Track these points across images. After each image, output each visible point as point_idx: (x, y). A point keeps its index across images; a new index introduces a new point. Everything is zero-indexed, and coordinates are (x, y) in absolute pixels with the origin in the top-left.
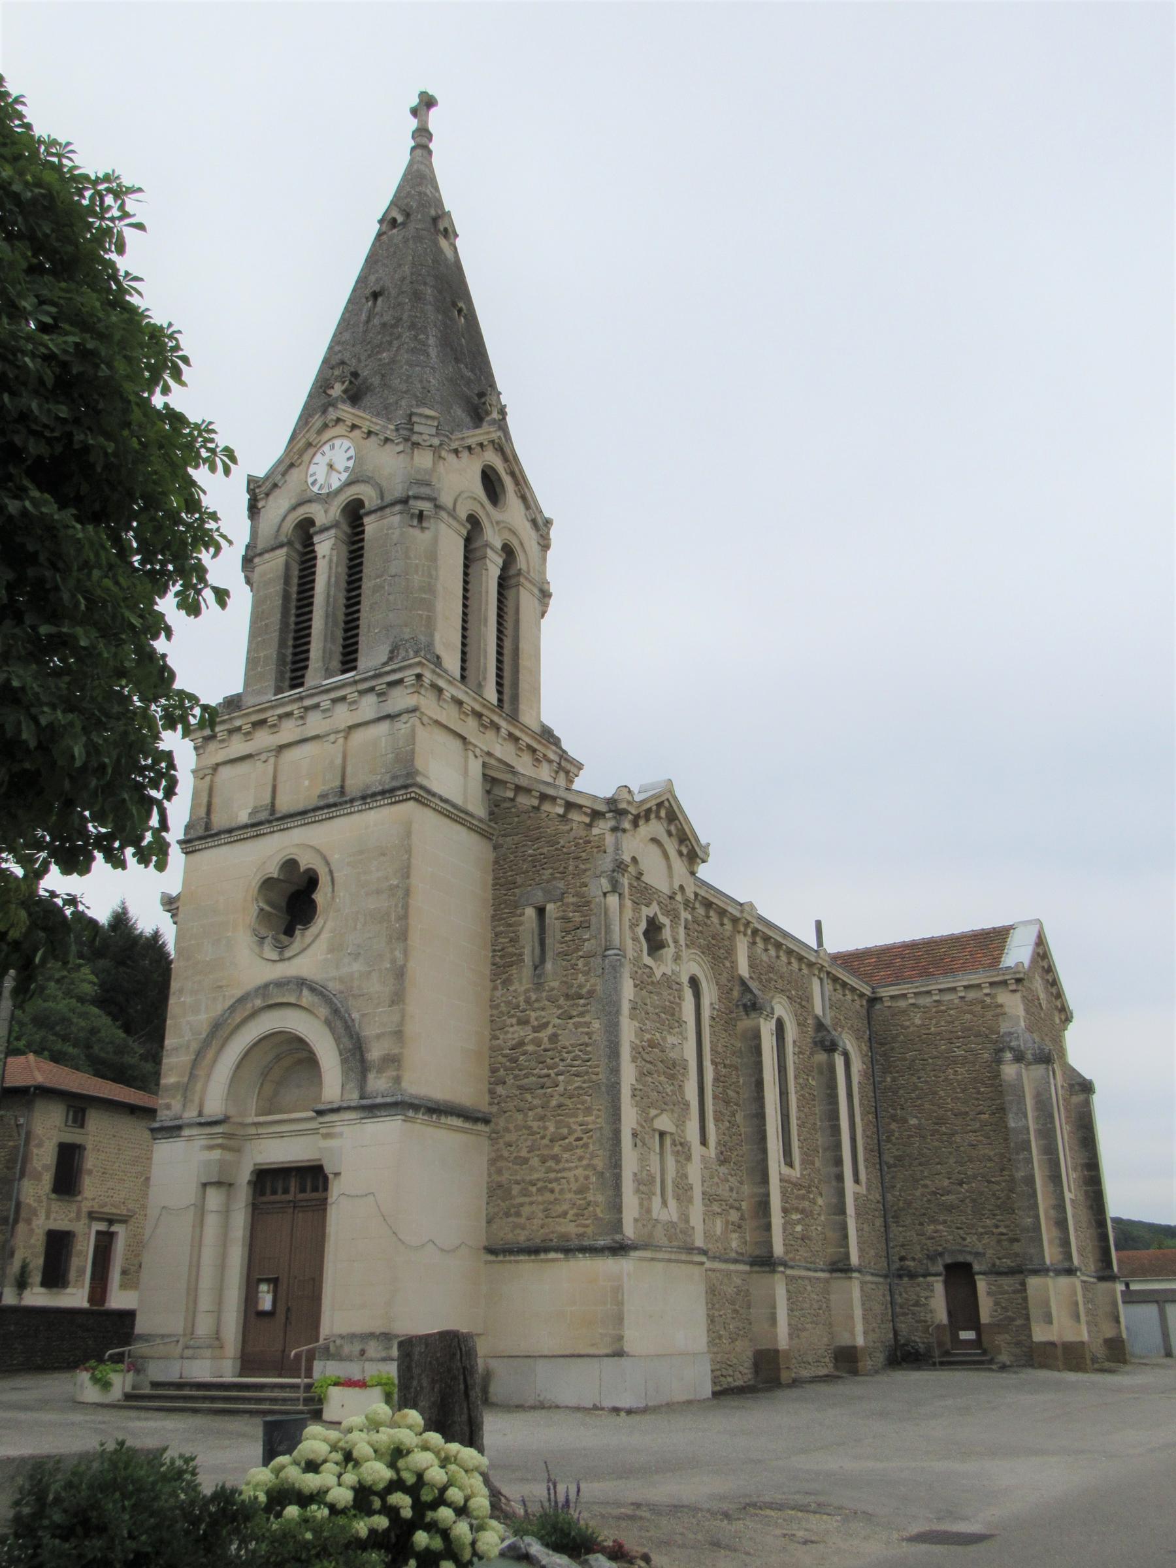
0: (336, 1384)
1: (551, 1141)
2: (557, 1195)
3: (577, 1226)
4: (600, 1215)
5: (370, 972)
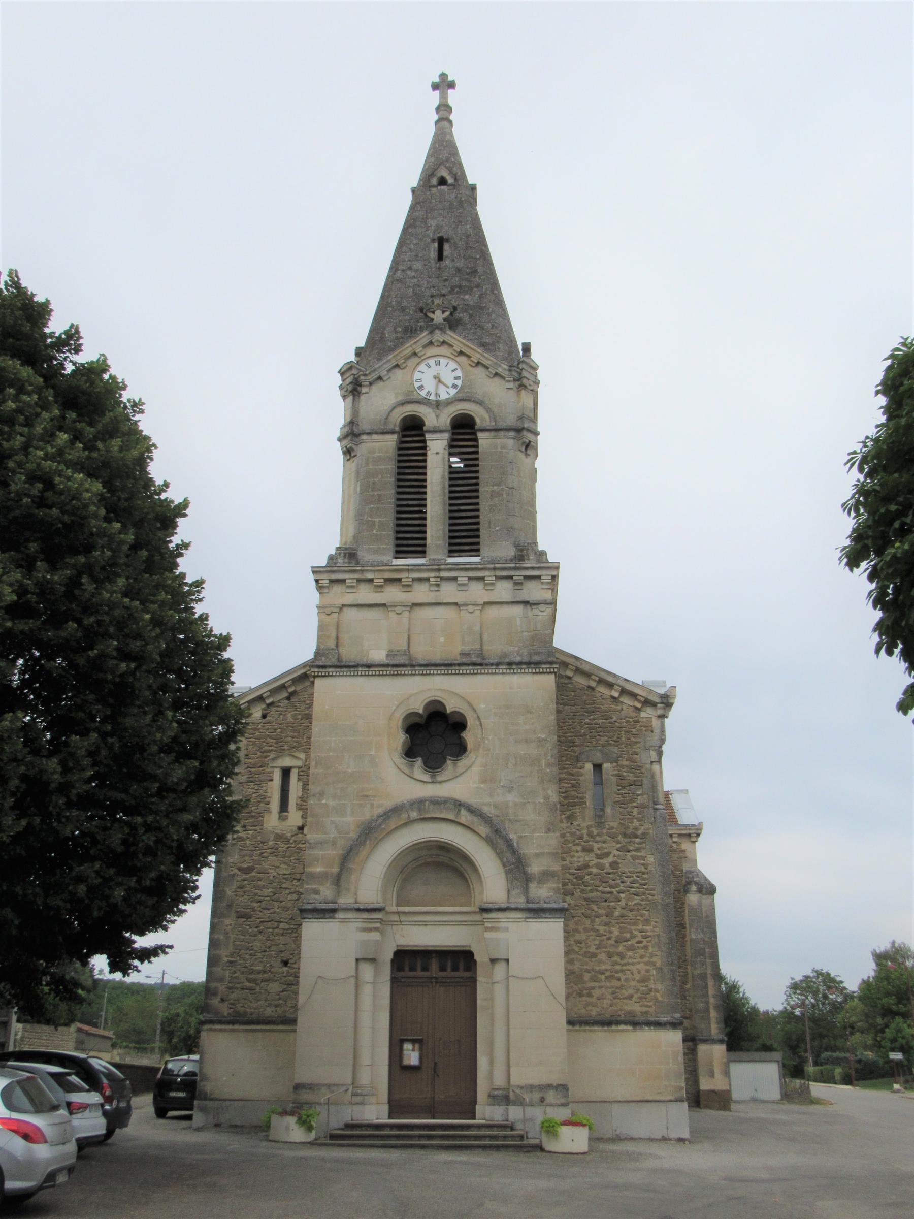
0: (562, 1124)
1: (616, 942)
2: (623, 982)
3: (641, 1006)
4: (660, 999)
5: (525, 804)
